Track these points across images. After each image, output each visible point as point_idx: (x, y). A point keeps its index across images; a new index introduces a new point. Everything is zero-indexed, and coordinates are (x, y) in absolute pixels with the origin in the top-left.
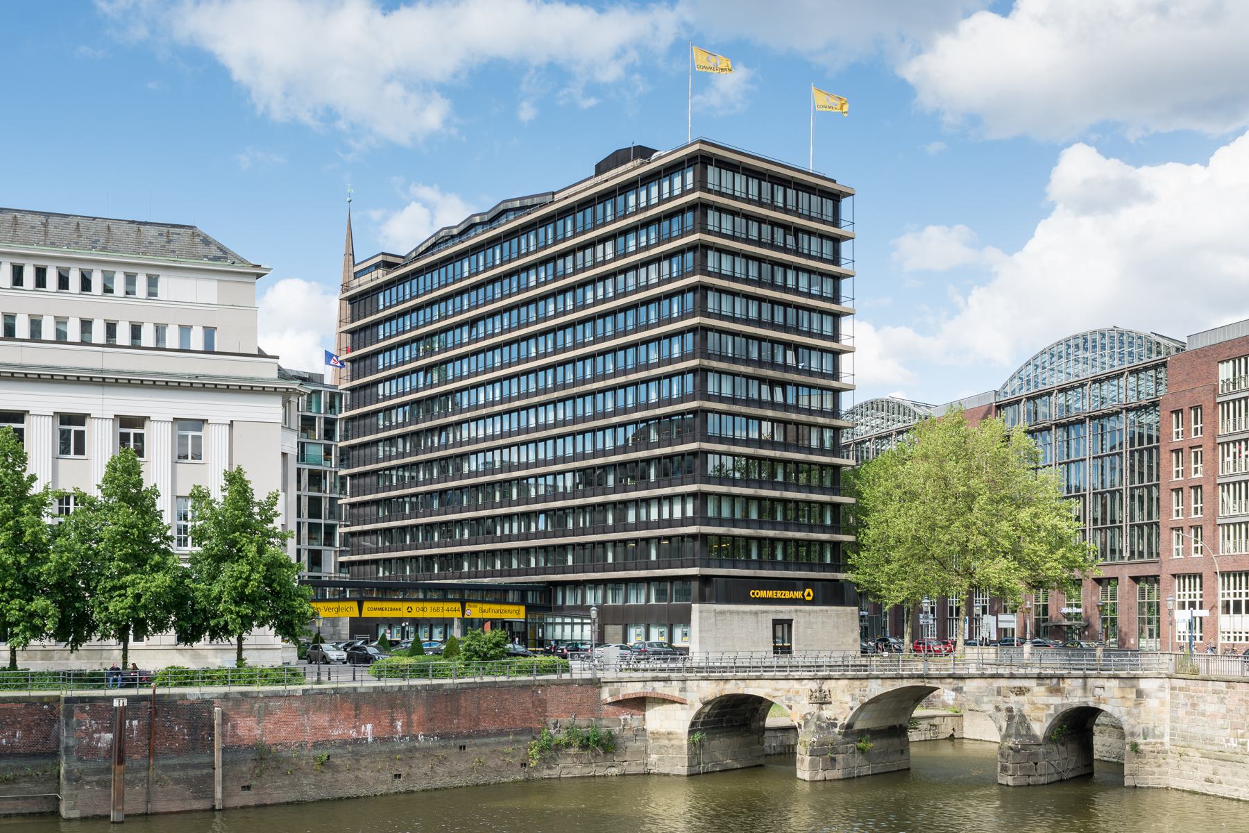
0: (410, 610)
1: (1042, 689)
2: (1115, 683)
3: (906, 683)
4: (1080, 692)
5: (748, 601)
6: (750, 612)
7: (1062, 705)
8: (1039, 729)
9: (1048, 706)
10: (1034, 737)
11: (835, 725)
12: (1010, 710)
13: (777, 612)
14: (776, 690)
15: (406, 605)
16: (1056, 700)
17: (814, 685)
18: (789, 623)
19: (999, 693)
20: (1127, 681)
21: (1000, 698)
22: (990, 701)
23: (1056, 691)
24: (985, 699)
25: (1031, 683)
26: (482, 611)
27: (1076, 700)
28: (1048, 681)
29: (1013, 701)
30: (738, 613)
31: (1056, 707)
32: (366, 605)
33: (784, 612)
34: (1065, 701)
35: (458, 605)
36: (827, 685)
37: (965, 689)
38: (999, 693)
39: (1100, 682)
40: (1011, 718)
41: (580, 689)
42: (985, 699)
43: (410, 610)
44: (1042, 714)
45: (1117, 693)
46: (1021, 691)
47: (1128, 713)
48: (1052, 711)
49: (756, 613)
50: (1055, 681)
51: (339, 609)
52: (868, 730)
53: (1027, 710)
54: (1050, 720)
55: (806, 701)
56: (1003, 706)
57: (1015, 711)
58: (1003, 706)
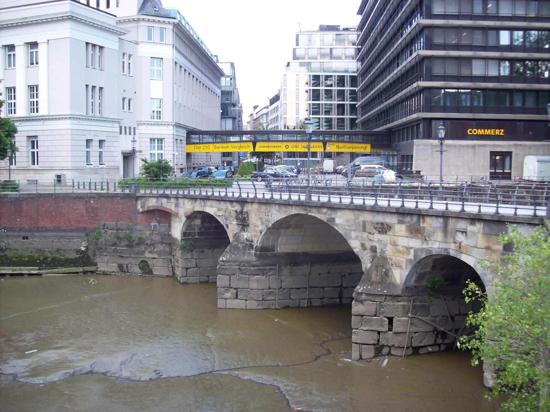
0: (287, 147)
1: (403, 227)
2: (478, 227)
3: (294, 211)
4: (439, 236)
5: (465, 137)
6: (468, 146)
7: (422, 250)
8: (399, 276)
9: (408, 249)
10: (393, 285)
11: (251, 246)
12: (374, 249)
13: (494, 146)
14: (219, 210)
15: (285, 144)
16: (416, 243)
17: (238, 207)
18: (510, 154)
19: (364, 230)
20: (494, 226)
21: (365, 235)
23: (415, 231)
24: (353, 234)
26: (338, 147)
27: (436, 245)
28: (408, 219)
30: (455, 146)
31: (416, 251)
32: (258, 144)
33: (503, 146)
34: (424, 246)
35: (321, 144)
36: (248, 208)
37: (337, 221)
39: (462, 225)
40: (374, 258)
41: (121, 201)
42: (353, 234)
43: (287, 147)
44: (402, 259)
45: (481, 242)
46: (384, 229)
47: (494, 271)
48: (411, 257)
49: (474, 146)
50: (415, 218)
51: (240, 147)
52: (305, 254)
53: (389, 251)
54: (410, 267)
56: (368, 245)
57: (378, 250)
58: (368, 245)
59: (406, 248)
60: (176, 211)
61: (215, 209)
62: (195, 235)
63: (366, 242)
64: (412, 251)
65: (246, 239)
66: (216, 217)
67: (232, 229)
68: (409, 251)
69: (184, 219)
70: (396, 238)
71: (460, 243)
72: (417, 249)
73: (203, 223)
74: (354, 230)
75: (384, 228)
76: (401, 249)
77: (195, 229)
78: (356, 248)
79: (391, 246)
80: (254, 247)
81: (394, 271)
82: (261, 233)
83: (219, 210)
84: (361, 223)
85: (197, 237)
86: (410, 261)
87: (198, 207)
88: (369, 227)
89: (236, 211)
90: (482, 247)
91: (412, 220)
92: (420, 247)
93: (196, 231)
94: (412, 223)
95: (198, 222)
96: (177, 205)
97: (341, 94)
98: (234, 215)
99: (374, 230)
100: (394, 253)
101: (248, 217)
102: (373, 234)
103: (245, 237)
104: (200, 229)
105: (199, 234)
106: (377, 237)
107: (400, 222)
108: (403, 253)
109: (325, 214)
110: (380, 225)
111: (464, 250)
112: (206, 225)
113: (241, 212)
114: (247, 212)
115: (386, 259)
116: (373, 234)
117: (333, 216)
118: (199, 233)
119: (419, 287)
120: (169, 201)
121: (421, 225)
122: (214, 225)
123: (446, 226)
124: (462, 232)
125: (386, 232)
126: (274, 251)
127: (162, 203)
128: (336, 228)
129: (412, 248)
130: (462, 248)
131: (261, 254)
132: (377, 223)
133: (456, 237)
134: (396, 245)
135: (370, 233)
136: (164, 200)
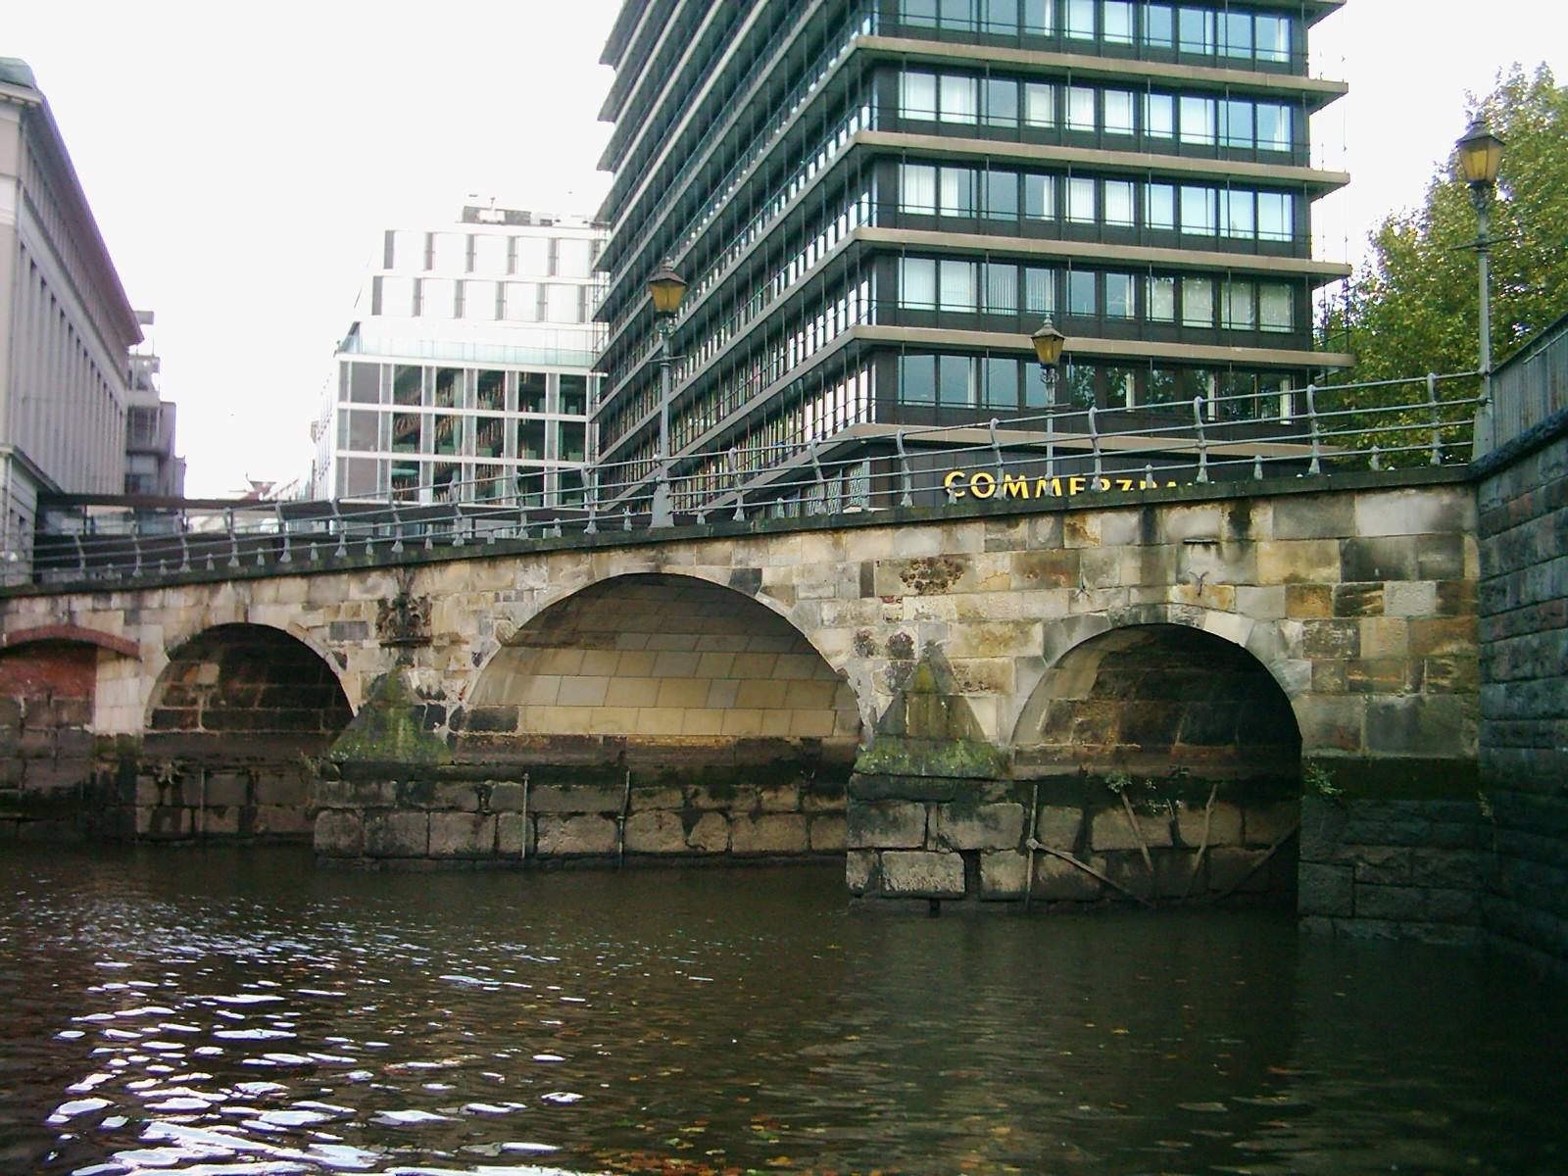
1: (1004, 561)
7: (1071, 622)
9: (1022, 626)
12: (900, 648)
14: (310, 606)
16: (1050, 604)
19: (867, 590)
21: (871, 604)
22: (840, 621)
25: (972, 537)
28: (1022, 530)
29: (916, 614)
37: (767, 578)
38: (867, 590)
46: (936, 575)
50: (1045, 526)
53: (955, 647)
55: (372, 643)
57: (917, 649)
59: (1017, 623)
60: (132, 638)
61: (296, 609)
62: (194, 724)
63: (875, 629)
64: (1037, 631)
65: (419, 691)
66: (300, 636)
67: (359, 669)
68: (1025, 634)
69: (162, 661)
70: (976, 599)
71: (1200, 581)
72: (1055, 622)
73: (225, 677)
74: (831, 599)
75: (937, 574)
76: (998, 630)
77: (194, 702)
78: (838, 653)
79: (964, 627)
80: (448, 715)
81: (973, 705)
82: (477, 661)
83: (310, 606)
84: (856, 571)
85: (201, 729)
86: (1035, 662)
87: (224, 605)
88: (879, 576)
89: (382, 602)
90: (1274, 579)
91: (1034, 534)
92: (1064, 613)
93: (200, 707)
94: (1035, 544)
95: (209, 673)
96: (132, 617)
97: (531, 436)
98: (371, 615)
99: (903, 586)
100: (976, 648)
101: (426, 615)
102: (899, 601)
103: (415, 684)
104: (214, 701)
105: (211, 719)
106: (912, 605)
107: (992, 547)
108: (1004, 642)
109: (727, 560)
110: (922, 568)
111: (1214, 601)
112: (237, 685)
113: (401, 604)
114: (423, 599)
115: (943, 669)
116: (899, 601)
117: (753, 565)
118: (205, 714)
119: (1055, 752)
120: (100, 605)
121: (1067, 544)
122: (263, 687)
123: (1149, 531)
124: (1206, 545)
125: (944, 585)
126: (514, 728)
127: (71, 614)
128: (765, 600)
129: (1036, 621)
130: (1206, 592)
131: (472, 739)
132: (915, 562)
133: (1183, 565)
134: (980, 623)
135: (888, 599)
136: (81, 604)
